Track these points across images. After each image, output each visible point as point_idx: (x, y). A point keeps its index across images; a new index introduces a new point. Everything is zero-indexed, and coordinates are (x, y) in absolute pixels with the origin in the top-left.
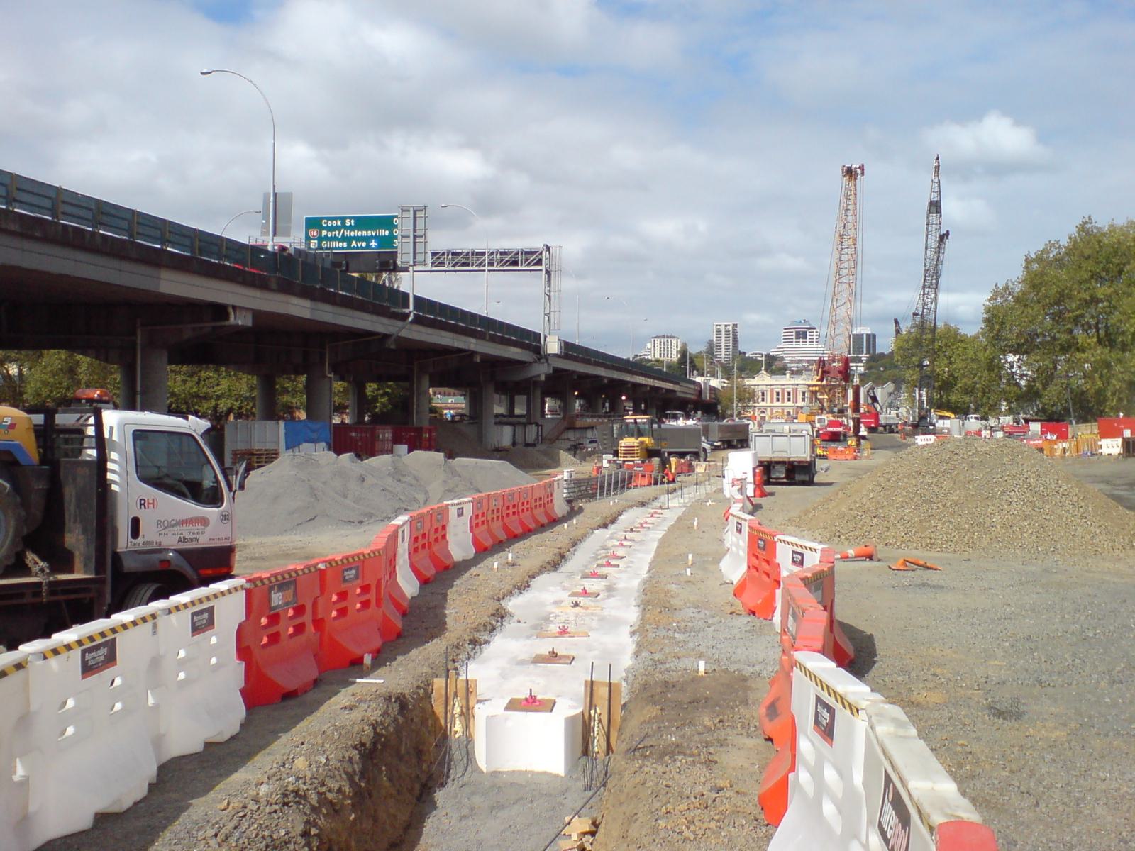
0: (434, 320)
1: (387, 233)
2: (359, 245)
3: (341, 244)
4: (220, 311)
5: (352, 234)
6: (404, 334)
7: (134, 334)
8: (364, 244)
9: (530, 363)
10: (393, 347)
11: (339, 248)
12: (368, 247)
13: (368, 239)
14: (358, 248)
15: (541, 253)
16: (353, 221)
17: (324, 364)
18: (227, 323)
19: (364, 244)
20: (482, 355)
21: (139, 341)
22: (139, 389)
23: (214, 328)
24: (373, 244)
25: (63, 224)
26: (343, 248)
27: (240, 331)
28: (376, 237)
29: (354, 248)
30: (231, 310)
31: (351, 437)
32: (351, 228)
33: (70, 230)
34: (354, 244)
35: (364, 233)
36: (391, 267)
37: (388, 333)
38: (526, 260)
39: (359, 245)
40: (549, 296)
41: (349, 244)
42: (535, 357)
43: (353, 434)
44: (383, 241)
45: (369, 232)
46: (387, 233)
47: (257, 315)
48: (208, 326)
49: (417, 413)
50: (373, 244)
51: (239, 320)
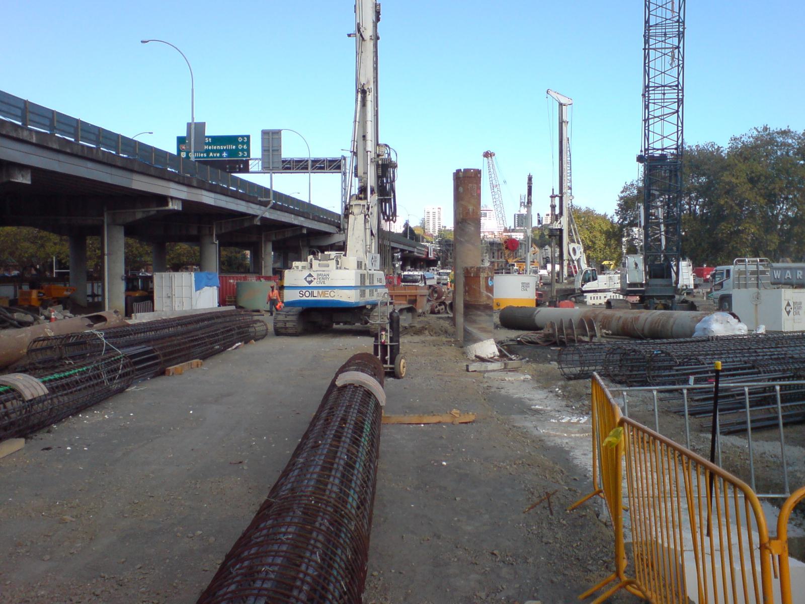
0: (282, 206)
1: (234, 147)
2: (215, 155)
3: (202, 155)
4: (163, 200)
5: (210, 148)
6: (267, 215)
7: (103, 215)
8: (218, 155)
9: (334, 234)
10: (259, 223)
11: (201, 157)
12: (221, 156)
13: (221, 152)
14: (214, 157)
15: (340, 161)
16: (210, 139)
17: (212, 235)
18: (167, 208)
19: (218, 155)
20: (308, 229)
21: (105, 220)
22: (106, 252)
23: (158, 211)
24: (225, 154)
25: (83, 146)
26: (204, 157)
27: (174, 213)
28: (226, 150)
29: (211, 157)
30: (170, 200)
31: (230, 283)
32: (209, 144)
33: (85, 148)
34: (211, 154)
35: (218, 147)
36: (238, 170)
37: (254, 214)
38: (330, 166)
39: (215, 155)
40: (345, 189)
41: (208, 155)
42: (337, 230)
43: (232, 281)
44: (231, 153)
45: (222, 148)
46: (234, 147)
47: (185, 202)
48: (153, 210)
49: (265, 267)
50: (225, 154)
51: (174, 206)
